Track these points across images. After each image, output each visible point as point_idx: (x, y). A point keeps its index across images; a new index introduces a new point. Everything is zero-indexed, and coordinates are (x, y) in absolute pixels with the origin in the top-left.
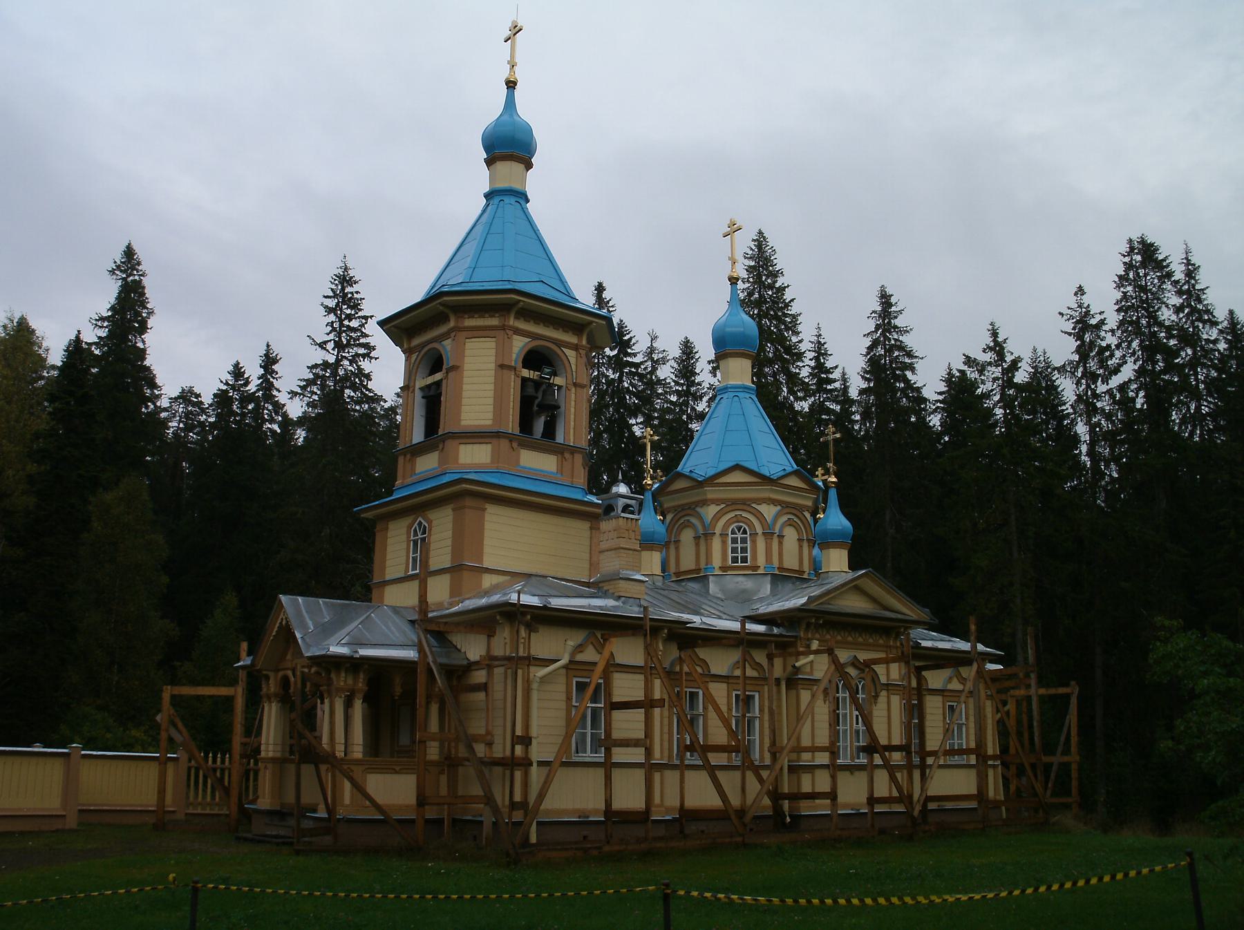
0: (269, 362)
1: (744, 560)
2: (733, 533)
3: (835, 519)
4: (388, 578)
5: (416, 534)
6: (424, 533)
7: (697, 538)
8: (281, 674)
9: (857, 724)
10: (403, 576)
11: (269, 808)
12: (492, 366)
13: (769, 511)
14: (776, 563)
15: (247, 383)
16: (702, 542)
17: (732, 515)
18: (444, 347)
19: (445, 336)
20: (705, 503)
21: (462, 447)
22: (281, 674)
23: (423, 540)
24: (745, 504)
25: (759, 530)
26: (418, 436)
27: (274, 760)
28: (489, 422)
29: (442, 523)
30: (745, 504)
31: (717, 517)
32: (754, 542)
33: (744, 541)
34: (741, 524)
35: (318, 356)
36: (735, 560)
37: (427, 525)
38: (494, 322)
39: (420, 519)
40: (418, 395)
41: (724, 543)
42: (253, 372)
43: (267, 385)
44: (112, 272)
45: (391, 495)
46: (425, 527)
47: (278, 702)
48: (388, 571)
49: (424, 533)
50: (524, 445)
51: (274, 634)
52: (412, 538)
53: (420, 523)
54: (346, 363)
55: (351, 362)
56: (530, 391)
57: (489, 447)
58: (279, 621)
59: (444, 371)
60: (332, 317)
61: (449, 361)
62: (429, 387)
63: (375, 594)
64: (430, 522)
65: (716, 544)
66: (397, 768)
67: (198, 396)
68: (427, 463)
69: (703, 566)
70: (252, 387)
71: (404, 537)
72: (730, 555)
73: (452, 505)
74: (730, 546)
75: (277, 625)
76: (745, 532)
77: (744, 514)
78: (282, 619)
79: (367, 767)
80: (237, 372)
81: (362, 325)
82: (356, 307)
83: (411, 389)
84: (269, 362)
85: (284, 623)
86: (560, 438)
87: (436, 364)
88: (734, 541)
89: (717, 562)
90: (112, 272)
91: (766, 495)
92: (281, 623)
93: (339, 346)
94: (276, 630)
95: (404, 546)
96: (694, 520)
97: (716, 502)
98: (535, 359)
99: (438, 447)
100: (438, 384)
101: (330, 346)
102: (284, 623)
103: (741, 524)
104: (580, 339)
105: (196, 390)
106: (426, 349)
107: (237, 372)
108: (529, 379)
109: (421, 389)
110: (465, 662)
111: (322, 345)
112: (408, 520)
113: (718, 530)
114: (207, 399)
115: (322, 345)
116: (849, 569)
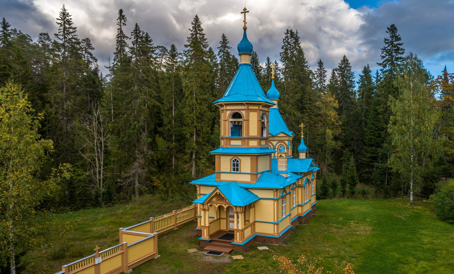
5: (234, 161)
10: (229, 171)
13: (287, 142)
17: (279, 144)
21: (250, 141)
23: (237, 165)
24: (282, 141)
28: (256, 135)
30: (282, 141)
38: (257, 108)
53: (236, 160)
57: (256, 141)
64: (240, 160)
71: (229, 162)
78: (217, 193)
85: (218, 194)
91: (287, 139)
97: (276, 140)
113: (277, 147)
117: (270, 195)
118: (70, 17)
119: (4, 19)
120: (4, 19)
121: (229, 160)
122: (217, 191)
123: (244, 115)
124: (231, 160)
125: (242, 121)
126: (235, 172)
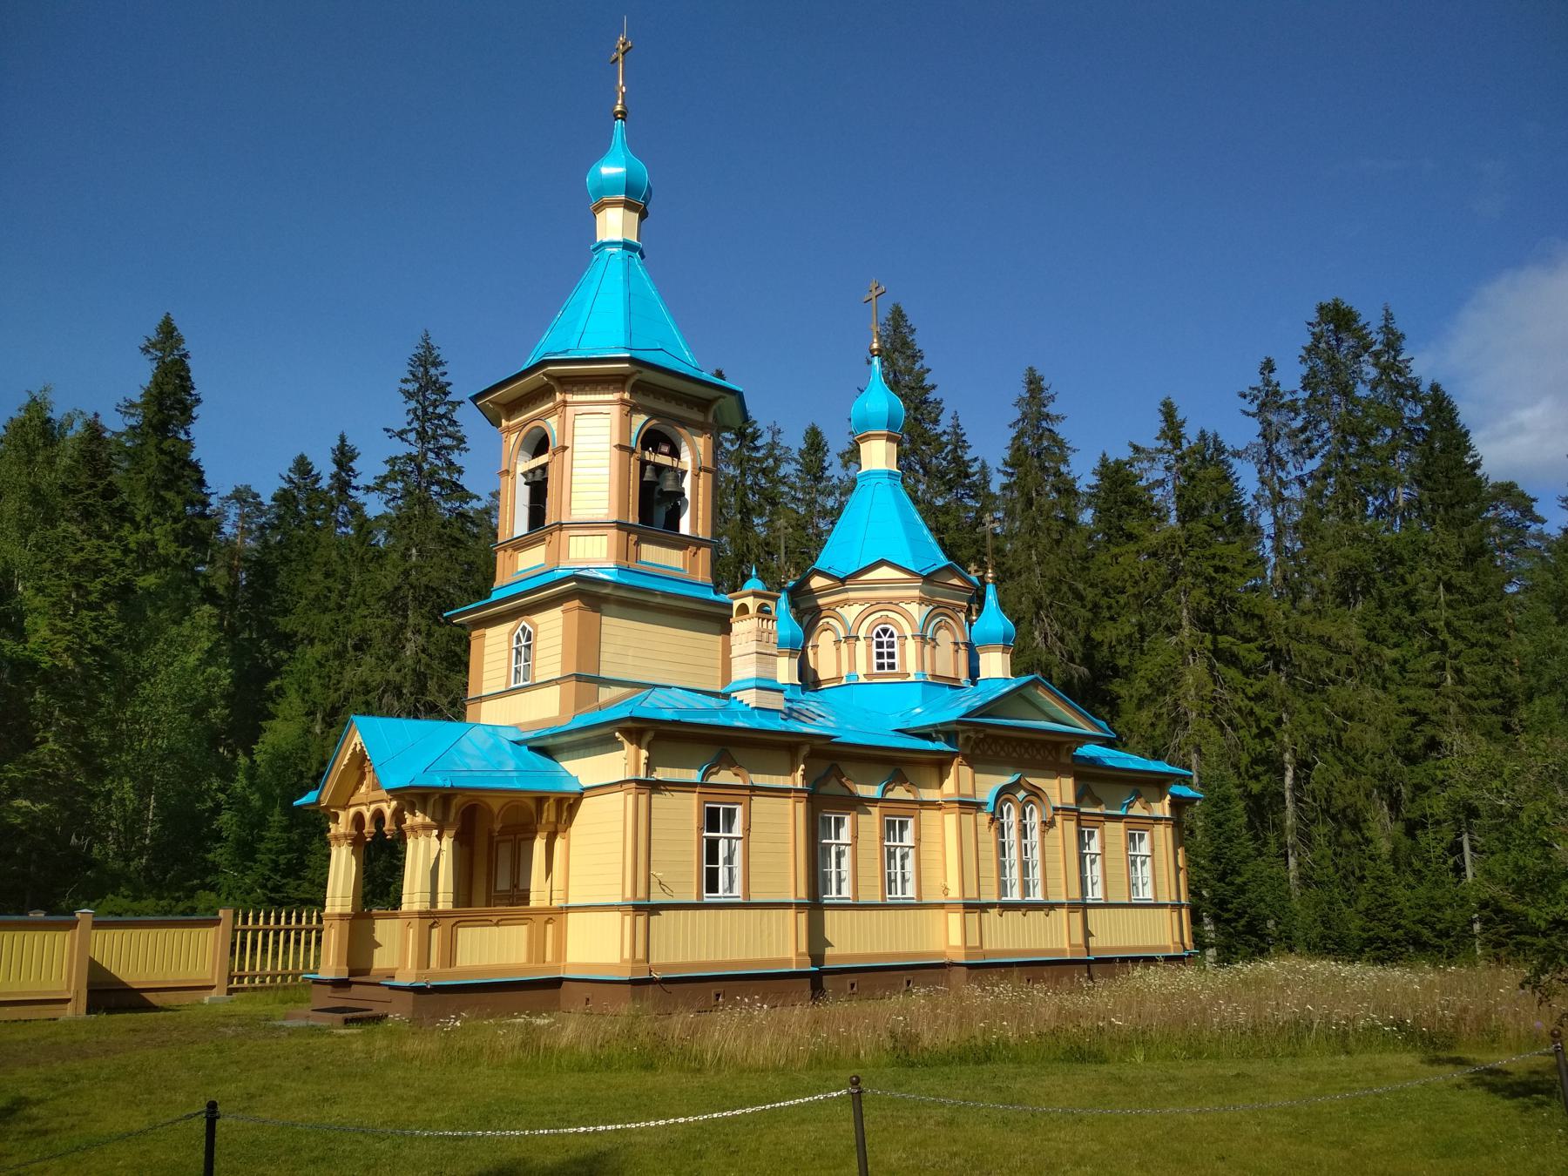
0: (344, 457)
1: (892, 666)
2: (878, 635)
3: (993, 620)
4: (484, 694)
6: (529, 639)
7: (837, 642)
8: (352, 811)
9: (1026, 855)
10: (503, 689)
11: (333, 977)
12: (607, 447)
14: (928, 671)
15: (317, 479)
16: (844, 646)
18: (549, 426)
19: (549, 413)
20: (846, 602)
22: (352, 811)
23: (528, 647)
25: (908, 632)
26: (521, 527)
27: (342, 916)
29: (551, 626)
31: (861, 619)
32: (903, 645)
33: (891, 645)
34: (888, 626)
35: (400, 449)
36: (881, 666)
37: (532, 630)
39: (524, 623)
40: (521, 480)
41: (869, 646)
42: (325, 468)
43: (343, 484)
44: (145, 350)
45: (487, 598)
46: (529, 633)
47: (351, 844)
48: (485, 685)
49: (529, 639)
50: (644, 539)
51: (345, 763)
52: (515, 646)
53: (524, 629)
54: (431, 455)
55: (438, 455)
56: (649, 475)
58: (352, 747)
59: (550, 452)
60: (413, 404)
61: (554, 442)
62: (533, 471)
63: (470, 709)
65: (861, 646)
66: (495, 919)
67: (256, 496)
68: (532, 559)
69: (845, 673)
70: (325, 483)
71: (505, 646)
72: (875, 661)
73: (561, 608)
74: (875, 650)
75: (350, 751)
76: (892, 635)
77: (891, 614)
79: (458, 919)
80: (303, 466)
81: (450, 411)
82: (443, 390)
83: (511, 475)
84: (344, 457)
85: (358, 748)
86: (685, 527)
87: (540, 445)
88: (880, 645)
89: (861, 669)
90: (145, 350)
92: (355, 748)
93: (422, 436)
94: (348, 756)
95: (505, 654)
96: (831, 621)
97: (856, 601)
98: (651, 439)
99: (544, 540)
100: (544, 468)
101: (412, 436)
102: (358, 749)
103: (888, 626)
104: (706, 416)
105: (255, 489)
106: (528, 427)
107: (303, 466)
108: (649, 462)
109: (524, 474)
110: (577, 789)
111: (401, 434)
112: (510, 625)
114: (267, 500)
115: (401, 434)
116: (1012, 675)
117: (620, 763)
118: (441, 369)
119: (343, 439)
120: (343, 439)
121: (506, 636)
122: (357, 739)
123: (555, 433)
124: (512, 633)
125: (547, 464)
126: (522, 683)
